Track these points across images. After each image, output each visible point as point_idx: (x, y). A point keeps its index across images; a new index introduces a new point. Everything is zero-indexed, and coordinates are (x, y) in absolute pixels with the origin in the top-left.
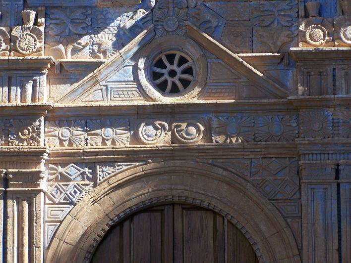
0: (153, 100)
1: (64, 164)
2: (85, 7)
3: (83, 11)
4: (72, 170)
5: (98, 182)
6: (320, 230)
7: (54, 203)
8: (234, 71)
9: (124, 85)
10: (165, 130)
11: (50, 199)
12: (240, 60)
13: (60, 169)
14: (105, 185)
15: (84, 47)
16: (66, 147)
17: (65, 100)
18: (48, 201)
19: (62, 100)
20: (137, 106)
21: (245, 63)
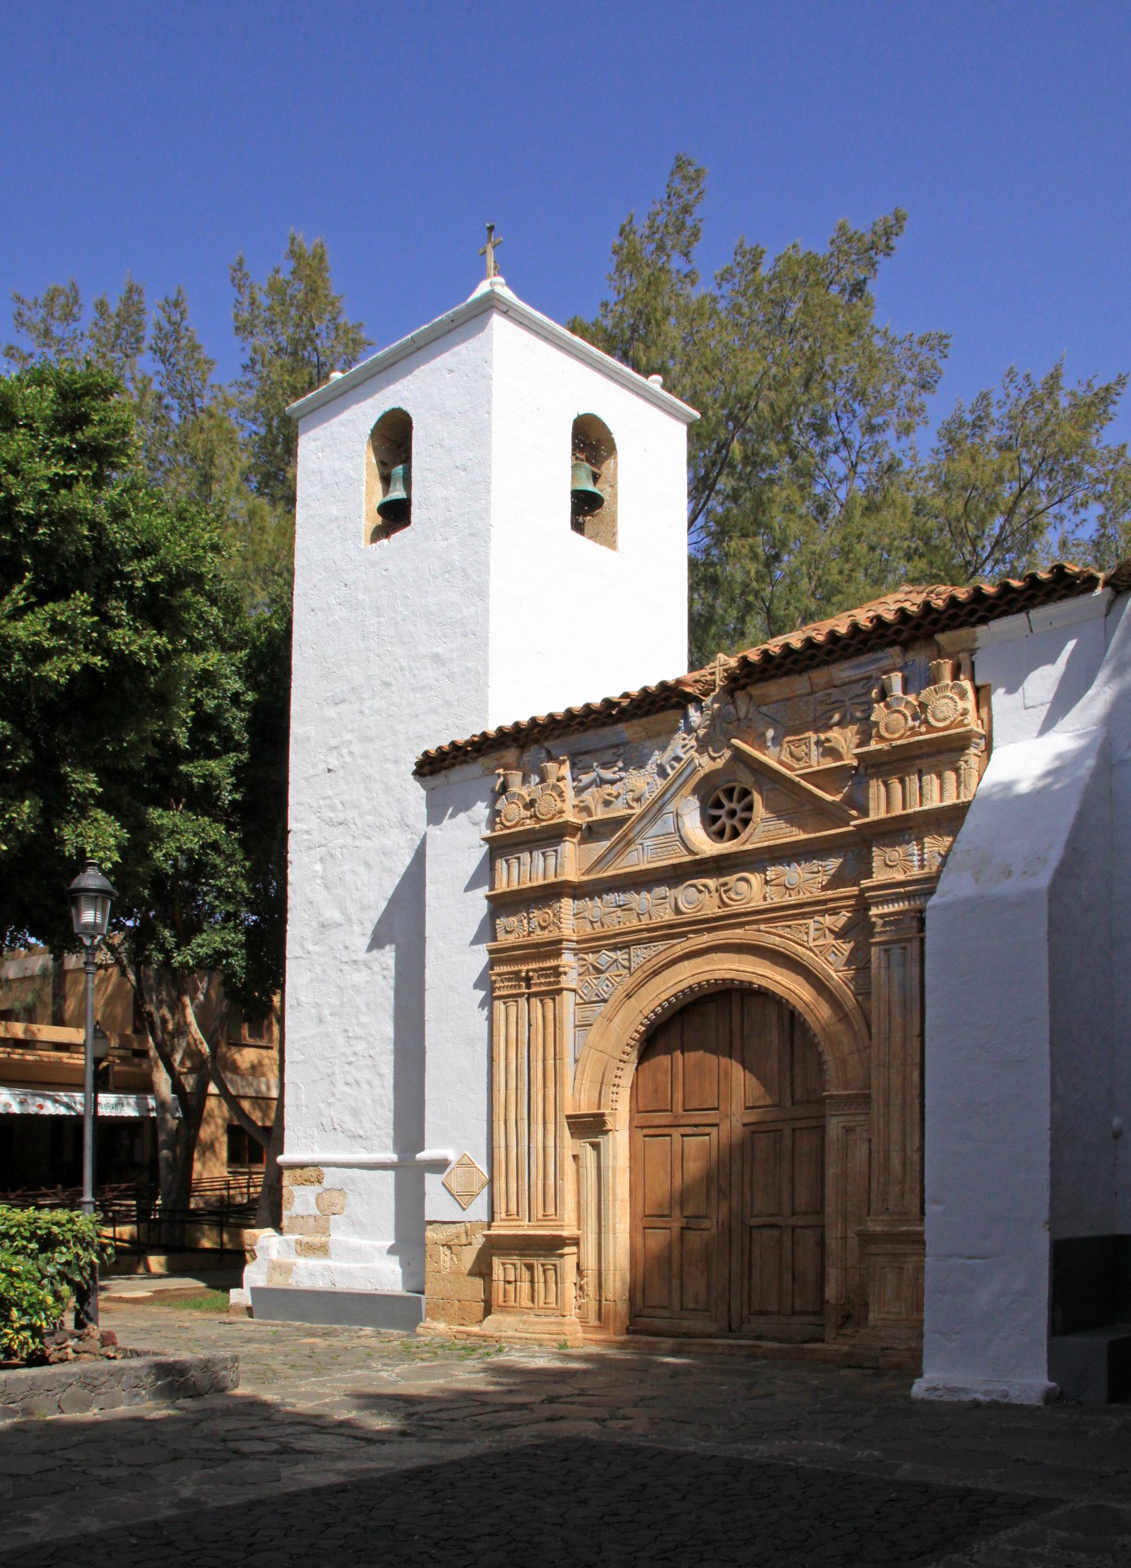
0: (696, 854)
1: (596, 950)
2: (616, 746)
3: (613, 750)
4: (606, 957)
5: (632, 970)
6: (896, 1009)
7: (585, 1003)
8: (795, 797)
9: (662, 840)
10: (710, 892)
11: (581, 998)
12: (797, 779)
13: (591, 957)
14: (639, 973)
15: (617, 797)
16: (597, 930)
17: (594, 871)
18: (579, 1001)
19: (588, 871)
20: (673, 865)
21: (803, 783)
